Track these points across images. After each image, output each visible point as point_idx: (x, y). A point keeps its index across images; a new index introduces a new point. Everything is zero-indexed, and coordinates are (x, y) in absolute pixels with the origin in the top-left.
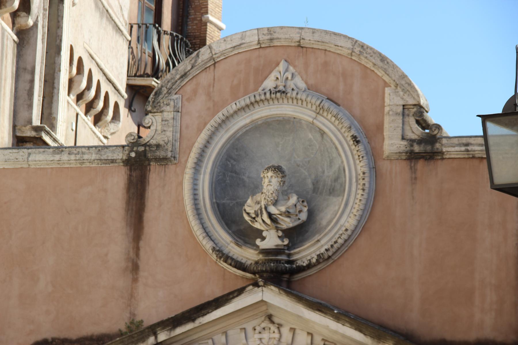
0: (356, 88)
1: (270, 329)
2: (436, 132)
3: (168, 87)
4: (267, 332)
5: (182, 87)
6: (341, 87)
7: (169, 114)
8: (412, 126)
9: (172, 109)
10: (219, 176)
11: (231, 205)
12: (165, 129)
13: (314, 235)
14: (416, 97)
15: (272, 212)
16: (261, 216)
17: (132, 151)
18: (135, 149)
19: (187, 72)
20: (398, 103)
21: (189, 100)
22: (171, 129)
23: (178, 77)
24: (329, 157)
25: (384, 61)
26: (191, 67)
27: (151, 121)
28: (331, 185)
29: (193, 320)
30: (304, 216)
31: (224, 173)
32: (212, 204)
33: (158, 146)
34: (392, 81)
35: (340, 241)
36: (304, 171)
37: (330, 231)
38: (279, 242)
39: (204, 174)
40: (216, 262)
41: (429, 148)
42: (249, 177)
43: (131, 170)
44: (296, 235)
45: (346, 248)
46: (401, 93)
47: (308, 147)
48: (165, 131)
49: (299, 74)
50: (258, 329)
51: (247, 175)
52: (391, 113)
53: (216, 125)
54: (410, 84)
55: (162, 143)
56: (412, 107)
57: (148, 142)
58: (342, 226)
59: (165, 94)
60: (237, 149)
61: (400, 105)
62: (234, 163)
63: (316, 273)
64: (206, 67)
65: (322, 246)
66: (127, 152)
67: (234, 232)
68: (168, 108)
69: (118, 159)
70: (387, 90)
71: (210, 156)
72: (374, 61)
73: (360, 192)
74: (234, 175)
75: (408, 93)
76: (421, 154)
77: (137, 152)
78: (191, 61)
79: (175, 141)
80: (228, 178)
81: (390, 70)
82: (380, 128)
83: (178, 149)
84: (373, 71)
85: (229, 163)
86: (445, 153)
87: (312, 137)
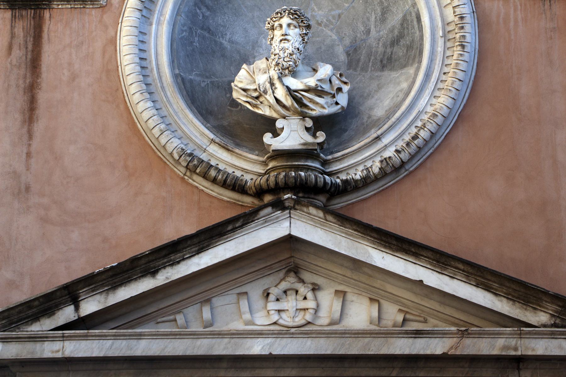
1: (297, 292)
4: (292, 297)
10: (183, 31)
11: (203, 85)
13: (366, 130)
15: (293, 87)
16: (273, 92)
28: (385, 52)
29: (154, 273)
30: (343, 100)
31: (190, 28)
32: (175, 76)
35: (424, 134)
36: (330, 33)
37: (399, 120)
39: (159, 23)
40: (183, 179)
42: (231, 41)
43: (14, 17)
44: (334, 128)
45: (431, 151)
50: (275, 292)
51: (228, 37)
58: (420, 113)
62: (208, 13)
63: (375, 194)
65: (386, 147)
67: (214, 127)
74: (207, 35)
80: (196, 39)
85: (198, 11)
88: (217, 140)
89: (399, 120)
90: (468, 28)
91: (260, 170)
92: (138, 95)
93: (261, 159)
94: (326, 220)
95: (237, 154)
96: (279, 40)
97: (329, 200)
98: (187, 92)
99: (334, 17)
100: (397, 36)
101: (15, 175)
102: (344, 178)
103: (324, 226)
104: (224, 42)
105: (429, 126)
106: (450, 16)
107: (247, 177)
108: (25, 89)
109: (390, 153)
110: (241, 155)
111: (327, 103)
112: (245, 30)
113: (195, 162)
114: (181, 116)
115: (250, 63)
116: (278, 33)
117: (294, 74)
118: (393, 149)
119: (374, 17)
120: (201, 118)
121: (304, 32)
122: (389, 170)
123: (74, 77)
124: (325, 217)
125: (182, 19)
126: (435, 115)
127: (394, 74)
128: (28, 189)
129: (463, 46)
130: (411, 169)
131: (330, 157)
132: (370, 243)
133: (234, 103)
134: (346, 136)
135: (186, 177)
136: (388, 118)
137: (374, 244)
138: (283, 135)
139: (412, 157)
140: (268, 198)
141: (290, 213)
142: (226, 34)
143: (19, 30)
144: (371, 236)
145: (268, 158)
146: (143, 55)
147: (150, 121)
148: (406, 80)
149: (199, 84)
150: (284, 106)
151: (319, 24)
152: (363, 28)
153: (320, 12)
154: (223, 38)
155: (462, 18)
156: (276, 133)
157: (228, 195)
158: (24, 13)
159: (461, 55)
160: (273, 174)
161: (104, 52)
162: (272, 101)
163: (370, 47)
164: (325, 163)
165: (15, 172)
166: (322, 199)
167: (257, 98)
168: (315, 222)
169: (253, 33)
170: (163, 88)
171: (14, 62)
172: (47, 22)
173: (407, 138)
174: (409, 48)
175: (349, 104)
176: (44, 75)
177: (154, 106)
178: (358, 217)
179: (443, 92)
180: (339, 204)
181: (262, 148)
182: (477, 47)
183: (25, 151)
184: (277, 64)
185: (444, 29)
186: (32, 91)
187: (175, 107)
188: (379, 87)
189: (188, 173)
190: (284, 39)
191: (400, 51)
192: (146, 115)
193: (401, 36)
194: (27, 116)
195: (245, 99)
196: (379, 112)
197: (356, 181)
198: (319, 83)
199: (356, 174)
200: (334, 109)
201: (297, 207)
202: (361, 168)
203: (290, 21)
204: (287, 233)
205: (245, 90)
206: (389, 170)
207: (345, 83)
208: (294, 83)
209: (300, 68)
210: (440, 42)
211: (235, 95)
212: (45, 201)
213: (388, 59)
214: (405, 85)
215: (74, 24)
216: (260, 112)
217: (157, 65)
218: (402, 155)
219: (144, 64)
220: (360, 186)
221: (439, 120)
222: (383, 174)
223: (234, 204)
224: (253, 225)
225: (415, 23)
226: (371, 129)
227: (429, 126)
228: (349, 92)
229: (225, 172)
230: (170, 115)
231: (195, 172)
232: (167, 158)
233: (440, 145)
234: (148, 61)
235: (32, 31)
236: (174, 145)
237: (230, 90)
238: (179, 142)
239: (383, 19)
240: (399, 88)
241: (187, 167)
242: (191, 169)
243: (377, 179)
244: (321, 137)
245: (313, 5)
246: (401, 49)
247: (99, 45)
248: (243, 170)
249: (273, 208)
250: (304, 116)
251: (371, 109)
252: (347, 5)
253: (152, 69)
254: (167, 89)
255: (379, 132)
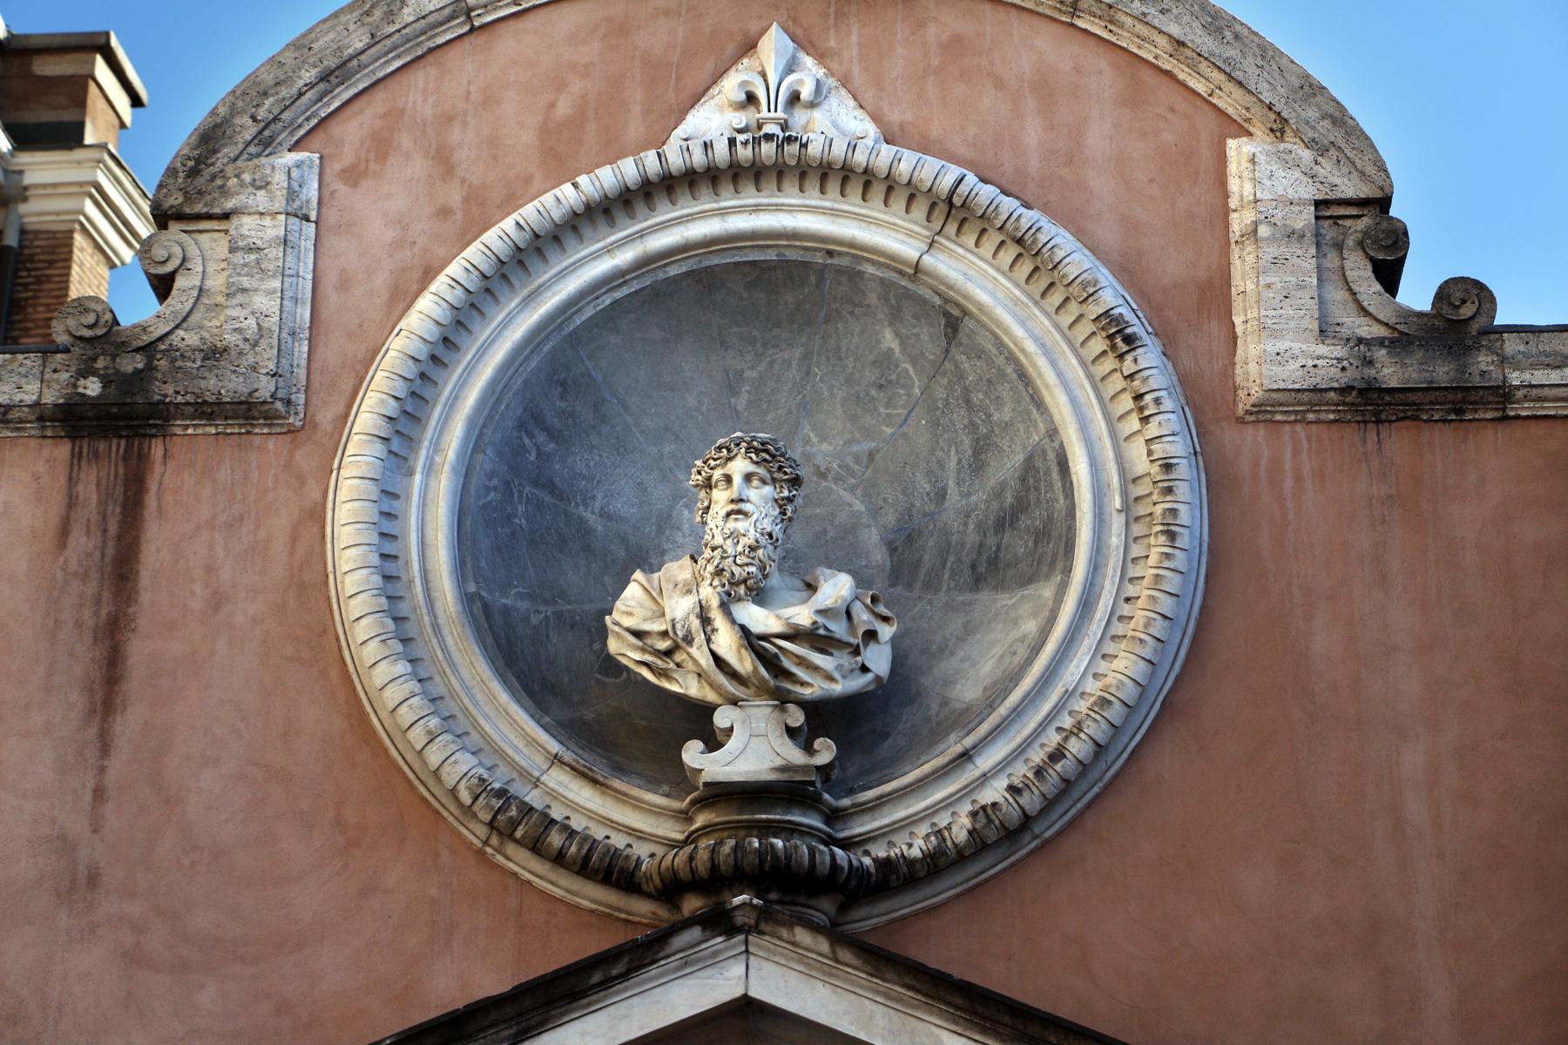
0: (1099, 138)
2: (1467, 311)
3: (262, 114)
5: (324, 120)
6: (1033, 133)
7: (267, 221)
8: (1356, 288)
9: (279, 204)
10: (488, 489)
11: (534, 620)
12: (245, 282)
13: (935, 734)
14: (1371, 170)
16: (708, 640)
17: (84, 374)
18: (100, 364)
19: (351, 58)
20: (1291, 194)
21: (353, 176)
22: (276, 284)
23: (309, 75)
24: (973, 426)
25: (1220, 30)
26: (366, 40)
27: (177, 251)
28: (981, 545)
30: (879, 660)
31: (507, 483)
32: (468, 600)
33: (214, 354)
34: (1257, 110)
35: (1078, 748)
36: (847, 497)
37: (1018, 712)
38: (796, 756)
39: (430, 470)
40: (480, 853)
41: (1443, 373)
42: (605, 515)
43: (76, 457)
44: (860, 729)
45: (1096, 790)
46: (1306, 155)
47: (873, 392)
48: (244, 290)
49: (845, 82)
51: (598, 504)
52: (1264, 231)
53: (473, 283)
54: (1340, 118)
55: (231, 339)
56: (1354, 211)
57: (162, 338)
58: (1068, 695)
59: (248, 144)
60: (564, 384)
61: (1302, 202)
63: (958, 896)
64: (431, 44)
65: (985, 778)
66: (64, 376)
67: (560, 724)
68: (261, 199)
69: (20, 405)
70: (1238, 150)
71: (454, 400)
72: (1175, 30)
73: (1157, 546)
74: (548, 499)
75: (1333, 151)
76: (1411, 397)
77: (106, 383)
78: (368, 13)
79: (293, 334)
80: (521, 508)
81: (1249, 69)
82: (1215, 295)
83: (302, 373)
84: (1168, 74)
85: (527, 441)
86: (1519, 394)
87: (895, 345)
88: (568, 756)
89: (1018, 712)
90: (1183, 491)
91: (672, 831)
92: (373, 644)
93: (677, 805)
94: (837, 961)
95: (616, 790)
96: (723, 513)
97: (843, 908)
98: (496, 638)
99: (857, 458)
100: (1012, 507)
101: (65, 845)
102: (882, 854)
103: (830, 975)
104: (588, 515)
105: (1090, 729)
106: (1140, 462)
107: (642, 850)
108: (95, 631)
109: (994, 793)
110: (626, 795)
111: (839, 668)
112: (642, 488)
113: (513, 812)
114: (480, 697)
115: (650, 568)
116: (720, 496)
117: (759, 595)
118: (1002, 783)
119: (954, 460)
120: (528, 702)
121: (786, 493)
122: (991, 835)
123: (217, 602)
124: (834, 952)
125: (485, 461)
126: (1104, 702)
127: (1004, 600)
128: (93, 879)
129: (1172, 536)
130: (1047, 835)
131: (846, 802)
132: (947, 1020)
133: (612, 666)
134: (885, 749)
135: (489, 850)
136: (991, 707)
137: (957, 1023)
138: (732, 745)
139: (1050, 804)
140: (692, 904)
141: (746, 942)
142: (594, 497)
143: (88, 490)
144: (948, 1004)
145: (693, 803)
146: (389, 548)
147: (404, 709)
148: (1035, 614)
149: (526, 619)
150: (733, 675)
151: (822, 475)
152: (927, 487)
153: (824, 446)
154: (586, 505)
155: (1168, 467)
156: (713, 742)
157: (591, 895)
158: (102, 446)
159: (1167, 556)
160: (703, 843)
161: (294, 540)
162: (706, 661)
163: (946, 532)
164: (835, 816)
165: (63, 838)
166: (826, 907)
167: (668, 653)
168: (808, 965)
169: (659, 494)
170: (436, 627)
171: (73, 566)
172: (158, 468)
173: (1037, 756)
174: (1042, 535)
175: (893, 670)
176: (145, 597)
177: (414, 674)
178: (916, 953)
179: (1123, 645)
180: (868, 919)
181: (678, 778)
182: (1206, 537)
183: (91, 785)
184: (719, 572)
185: (1124, 493)
186: (112, 635)
187: (465, 674)
188: (969, 631)
189: (494, 840)
190: (736, 510)
191: (1018, 544)
192: (392, 695)
193: (1021, 507)
194: (99, 697)
195: (638, 656)
196: (968, 692)
197: (911, 863)
198: (820, 620)
199: (910, 846)
200: (857, 683)
201: (763, 926)
202: (923, 829)
203: (752, 468)
204: (738, 992)
205: (638, 634)
206: (991, 835)
207: (886, 619)
208: (760, 619)
209: (775, 580)
210: (1117, 523)
211: (613, 646)
212: (136, 909)
213: (989, 562)
214: (1030, 627)
215: (224, 474)
216: (675, 688)
217: (424, 572)
218: (1025, 800)
219: (391, 568)
220: (922, 874)
221: (1115, 713)
222: (979, 844)
223: (605, 918)
224: (654, 971)
225: (1055, 476)
226: (947, 733)
227: (1090, 729)
228: (895, 641)
229: (586, 838)
230: (453, 694)
231: (511, 837)
232: (443, 800)
233: (1117, 775)
234: (401, 562)
235: (119, 490)
236: (460, 767)
237: (603, 633)
238: (473, 761)
239: (977, 464)
240: (1016, 634)
241: (491, 825)
242: (501, 829)
243: (962, 857)
244: (825, 751)
245: (807, 429)
246: (1020, 537)
247: (281, 522)
248: (632, 832)
249: (704, 930)
250: (782, 699)
251: (948, 682)
252: (889, 430)
253: (411, 582)
254: (446, 631)
255: (969, 741)
